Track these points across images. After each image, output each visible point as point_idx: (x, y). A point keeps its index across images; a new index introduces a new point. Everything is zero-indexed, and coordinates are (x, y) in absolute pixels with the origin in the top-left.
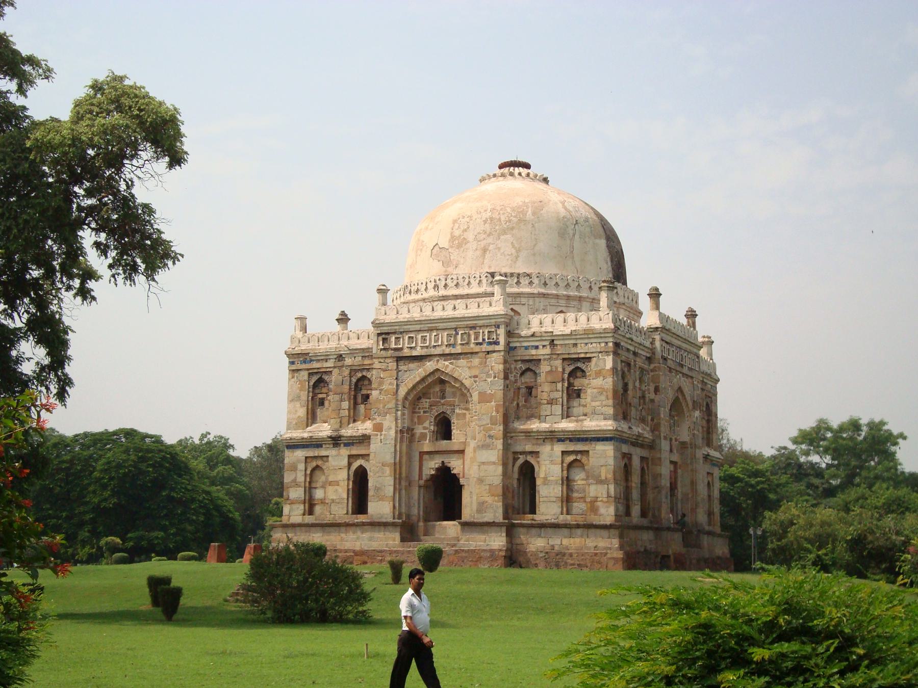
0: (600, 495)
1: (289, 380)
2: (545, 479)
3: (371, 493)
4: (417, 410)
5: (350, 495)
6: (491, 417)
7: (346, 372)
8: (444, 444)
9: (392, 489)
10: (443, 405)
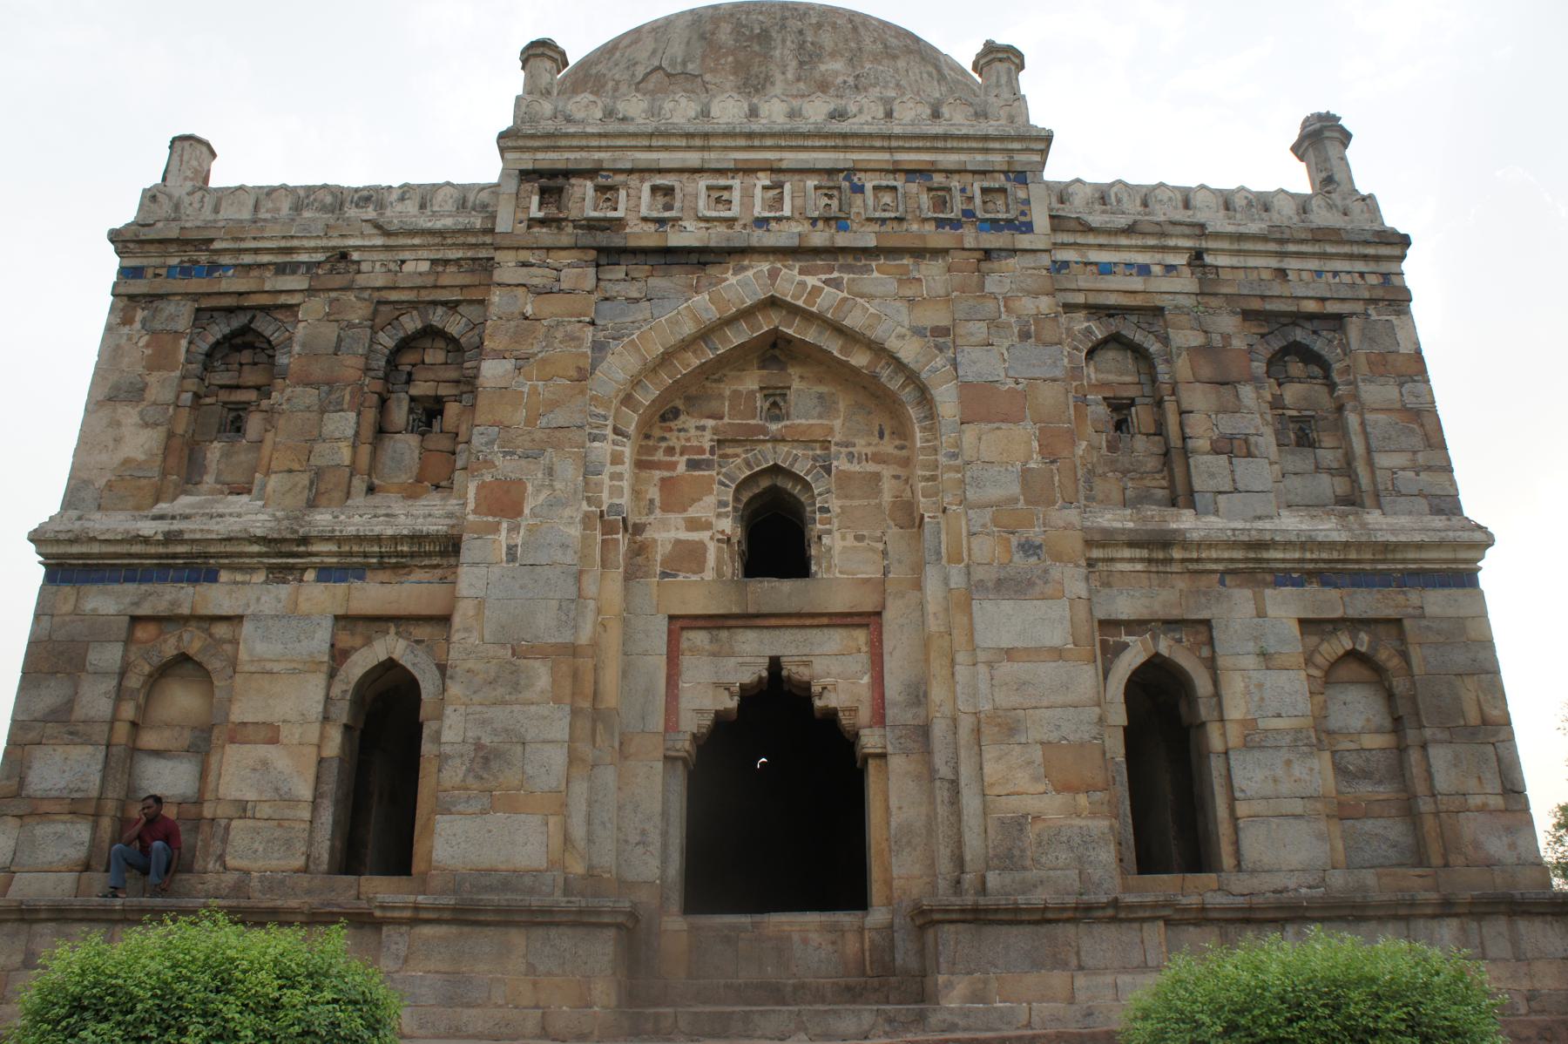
0: (1472, 784)
1: (109, 329)
2: (1249, 724)
4: (659, 456)
5: (330, 786)
6: (1026, 473)
7: (357, 311)
8: (778, 592)
9: (558, 757)
10: (776, 440)
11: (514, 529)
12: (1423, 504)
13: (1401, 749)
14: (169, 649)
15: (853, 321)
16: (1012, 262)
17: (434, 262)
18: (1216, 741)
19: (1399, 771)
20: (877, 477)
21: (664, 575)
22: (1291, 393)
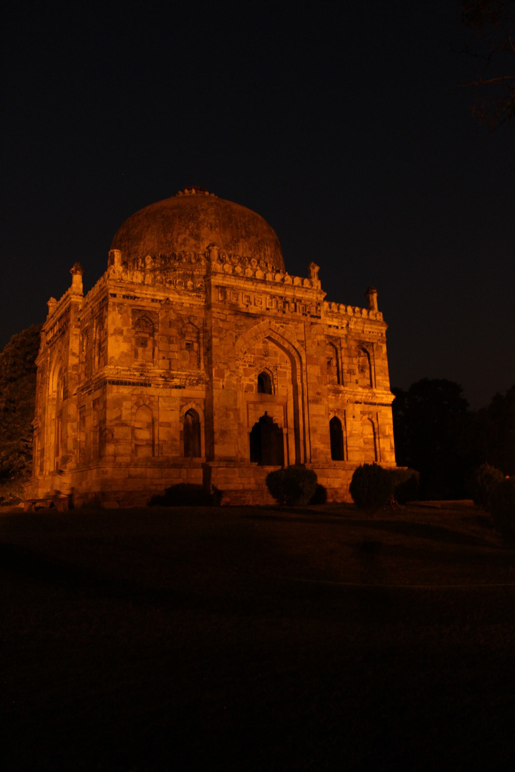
2: (351, 432)
3: (217, 436)
9: (236, 433)
10: (267, 361)
11: (223, 381)
12: (383, 389)
13: (375, 438)
15: (286, 337)
16: (316, 326)
17: (190, 304)
18: (344, 435)
20: (285, 373)
21: (245, 392)
22: (361, 359)
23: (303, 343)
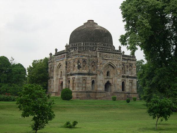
3: (99, 86)
14: (84, 79)
19: (132, 87)
23: (117, 65)
